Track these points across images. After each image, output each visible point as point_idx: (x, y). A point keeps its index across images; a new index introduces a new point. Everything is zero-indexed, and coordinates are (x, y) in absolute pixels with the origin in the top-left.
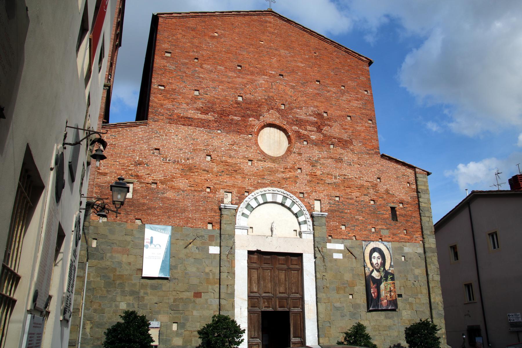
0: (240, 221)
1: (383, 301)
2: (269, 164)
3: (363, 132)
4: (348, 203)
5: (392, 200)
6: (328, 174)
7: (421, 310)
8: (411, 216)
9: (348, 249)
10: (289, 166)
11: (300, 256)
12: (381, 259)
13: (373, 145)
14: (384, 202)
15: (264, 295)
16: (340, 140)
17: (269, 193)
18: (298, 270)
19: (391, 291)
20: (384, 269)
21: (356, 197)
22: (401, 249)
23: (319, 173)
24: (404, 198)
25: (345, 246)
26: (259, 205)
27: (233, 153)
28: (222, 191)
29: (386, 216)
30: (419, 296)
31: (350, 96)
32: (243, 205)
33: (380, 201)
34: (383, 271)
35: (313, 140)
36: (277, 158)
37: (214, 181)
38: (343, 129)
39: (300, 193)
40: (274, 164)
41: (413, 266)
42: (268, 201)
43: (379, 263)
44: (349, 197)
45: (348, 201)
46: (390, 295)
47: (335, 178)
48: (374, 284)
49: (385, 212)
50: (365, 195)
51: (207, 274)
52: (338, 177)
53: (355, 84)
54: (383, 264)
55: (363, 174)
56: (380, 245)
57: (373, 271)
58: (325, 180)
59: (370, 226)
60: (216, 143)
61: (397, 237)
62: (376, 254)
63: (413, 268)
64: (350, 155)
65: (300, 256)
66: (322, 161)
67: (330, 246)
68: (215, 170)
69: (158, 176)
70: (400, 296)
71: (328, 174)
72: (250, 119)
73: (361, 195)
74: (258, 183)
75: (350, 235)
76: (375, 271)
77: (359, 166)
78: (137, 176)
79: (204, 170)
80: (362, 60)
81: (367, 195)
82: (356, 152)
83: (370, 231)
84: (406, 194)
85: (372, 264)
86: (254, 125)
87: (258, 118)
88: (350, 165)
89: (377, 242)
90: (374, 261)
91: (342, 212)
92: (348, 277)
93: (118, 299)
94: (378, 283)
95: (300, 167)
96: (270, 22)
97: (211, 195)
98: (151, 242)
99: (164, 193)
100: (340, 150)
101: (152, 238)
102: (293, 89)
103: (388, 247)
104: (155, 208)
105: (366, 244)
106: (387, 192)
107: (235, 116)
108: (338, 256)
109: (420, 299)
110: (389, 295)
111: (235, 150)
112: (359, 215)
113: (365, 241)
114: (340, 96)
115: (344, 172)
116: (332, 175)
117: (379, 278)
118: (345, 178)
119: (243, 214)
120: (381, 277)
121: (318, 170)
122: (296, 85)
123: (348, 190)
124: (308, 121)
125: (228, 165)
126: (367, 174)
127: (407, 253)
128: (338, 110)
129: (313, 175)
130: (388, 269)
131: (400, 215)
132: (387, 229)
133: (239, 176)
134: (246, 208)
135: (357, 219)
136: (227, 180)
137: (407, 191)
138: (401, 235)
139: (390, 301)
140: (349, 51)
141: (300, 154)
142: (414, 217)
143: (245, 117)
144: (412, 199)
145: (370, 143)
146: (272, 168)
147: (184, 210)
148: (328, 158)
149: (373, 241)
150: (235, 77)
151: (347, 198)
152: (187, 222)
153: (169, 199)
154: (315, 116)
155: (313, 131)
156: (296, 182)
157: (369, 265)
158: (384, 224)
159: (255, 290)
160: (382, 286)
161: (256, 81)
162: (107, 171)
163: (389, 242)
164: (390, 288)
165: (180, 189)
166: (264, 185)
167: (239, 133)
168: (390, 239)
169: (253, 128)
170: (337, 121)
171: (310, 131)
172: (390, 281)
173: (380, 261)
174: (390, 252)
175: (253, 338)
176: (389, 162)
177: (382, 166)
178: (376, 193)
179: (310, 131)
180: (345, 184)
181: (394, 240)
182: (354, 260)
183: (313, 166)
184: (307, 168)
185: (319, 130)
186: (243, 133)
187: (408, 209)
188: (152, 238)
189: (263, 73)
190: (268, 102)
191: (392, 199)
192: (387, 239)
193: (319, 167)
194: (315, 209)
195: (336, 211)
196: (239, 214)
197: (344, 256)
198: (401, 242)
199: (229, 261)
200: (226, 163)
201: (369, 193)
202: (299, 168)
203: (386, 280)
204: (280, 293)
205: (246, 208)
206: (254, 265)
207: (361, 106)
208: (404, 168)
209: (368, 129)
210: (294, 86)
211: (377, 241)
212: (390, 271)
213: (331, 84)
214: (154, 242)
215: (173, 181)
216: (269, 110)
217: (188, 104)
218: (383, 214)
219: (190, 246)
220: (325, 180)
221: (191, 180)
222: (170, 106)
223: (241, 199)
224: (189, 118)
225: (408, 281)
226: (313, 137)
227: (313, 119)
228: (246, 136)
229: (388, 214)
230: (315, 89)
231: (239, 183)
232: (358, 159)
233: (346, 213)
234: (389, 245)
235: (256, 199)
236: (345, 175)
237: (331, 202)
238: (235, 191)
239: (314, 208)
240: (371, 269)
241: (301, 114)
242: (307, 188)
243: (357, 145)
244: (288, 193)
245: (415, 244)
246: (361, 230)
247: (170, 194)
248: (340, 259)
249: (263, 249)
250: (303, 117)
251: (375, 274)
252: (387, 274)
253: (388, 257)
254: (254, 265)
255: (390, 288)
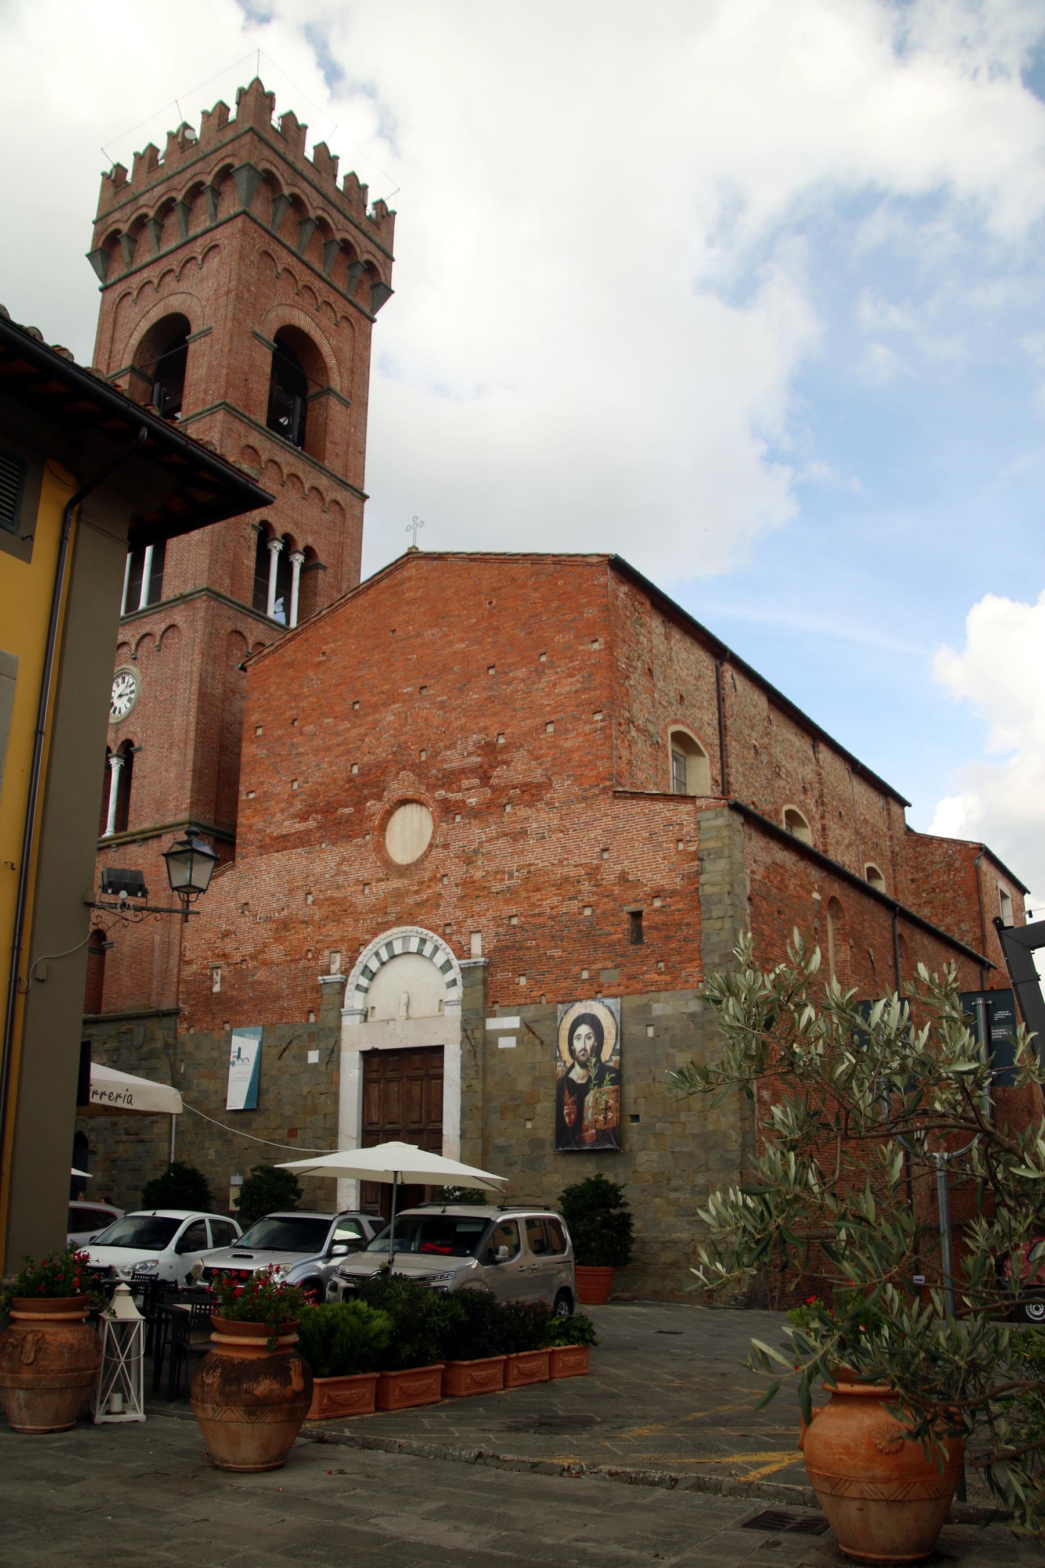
0: (354, 1000)
1: (587, 1131)
2: (396, 883)
3: (579, 749)
4: (535, 925)
5: (633, 895)
6: (497, 873)
7: (685, 1149)
8: (679, 925)
9: (526, 1025)
10: (427, 875)
11: (440, 1049)
12: (593, 1039)
13: (599, 773)
14: (612, 904)
15: (388, 1126)
16: (525, 788)
17: (412, 934)
18: (379, 1082)
19: (607, 1108)
20: (599, 1059)
21: (552, 908)
22: (647, 1008)
23: (478, 874)
24: (663, 882)
25: (522, 1020)
26: (383, 964)
27: (340, 880)
28: (326, 953)
29: (615, 937)
30: (683, 1117)
31: (557, 673)
32: (356, 971)
33: (605, 904)
34: (595, 1065)
35: (473, 808)
36: (408, 867)
37: (316, 938)
38: (534, 760)
39: (446, 925)
40: (402, 881)
41: (673, 1046)
42: (411, 950)
43: (588, 1048)
44: (536, 911)
45: (533, 920)
46: (605, 1118)
47: (511, 876)
48: (571, 1095)
49: (612, 929)
50: (570, 899)
51: (305, 1097)
52: (516, 874)
53: (570, 636)
54: (597, 1050)
55: (569, 852)
56: (597, 1008)
57: (573, 1066)
58: (489, 888)
59: (578, 968)
60: (318, 868)
61: (638, 982)
62: (584, 1030)
63: (672, 1051)
64: (543, 815)
65: (440, 1049)
66: (490, 847)
67: (493, 1024)
68: (317, 918)
69: (248, 949)
70: (635, 1118)
71: (497, 873)
72: (368, 804)
73: (563, 901)
74: (378, 924)
75: (533, 994)
76: (577, 1066)
77: (561, 835)
78: (225, 956)
79: (303, 922)
80: (592, 565)
81: (575, 898)
82: (557, 804)
83: (577, 978)
84: (671, 871)
85: (572, 1052)
86: (373, 815)
87: (379, 797)
88: (543, 838)
89: (590, 1002)
90: (578, 1045)
91: (521, 948)
92: (523, 1084)
93: (207, 1145)
94: (580, 1091)
95: (446, 871)
96: (409, 579)
97: (312, 963)
98: (239, 1057)
99: (253, 975)
100: (523, 812)
101: (240, 1049)
102: (442, 708)
103: (613, 1010)
104: (244, 1002)
105: (565, 1009)
106: (623, 878)
107: (347, 807)
108: (507, 1043)
109: (684, 1123)
110: (601, 1118)
111: (345, 872)
112: (555, 947)
113: (563, 1002)
114: (533, 683)
115: (530, 858)
116: (504, 872)
117: (583, 1081)
118: (529, 872)
119: (358, 987)
120: (589, 1080)
121: (478, 868)
122: (449, 698)
123: (538, 896)
124: (464, 769)
125: (333, 904)
126: (578, 848)
127: (660, 1018)
128: (527, 718)
129: (467, 883)
130: (607, 1058)
131: (650, 927)
132: (616, 967)
133: (349, 921)
134: (363, 973)
135: (552, 957)
136: (334, 931)
137: (673, 863)
138: (648, 976)
139: (602, 1131)
140: (560, 558)
141: (446, 846)
142: (688, 924)
143: (359, 804)
144: (686, 881)
145: (592, 770)
146: (399, 889)
147: (278, 997)
148: (497, 838)
149: (580, 1000)
150: (349, 729)
151: (532, 915)
152: (282, 1015)
153: (260, 983)
154: (479, 752)
155: (473, 788)
156: (438, 906)
157: (566, 1056)
158: (610, 958)
159: (375, 1119)
160: (589, 1099)
161: (380, 721)
162: (193, 956)
163: (616, 997)
164: (607, 1102)
165: (273, 963)
166: (386, 926)
167: (349, 838)
168: (622, 988)
169: (371, 821)
170: (522, 746)
171: (467, 789)
172: (608, 1087)
173: (590, 1044)
174: (614, 1018)
175: (370, 1203)
176: (634, 802)
177: (614, 818)
178: (595, 889)
179: (467, 789)
180: (530, 886)
181: (629, 990)
182: (539, 1046)
183: (468, 864)
184: (456, 870)
185: (485, 779)
186: (357, 836)
187: (673, 908)
188: (240, 1049)
189: (392, 698)
190: (399, 757)
191: (631, 894)
192: (614, 991)
193: (479, 863)
194: (472, 951)
195: (508, 948)
196: (350, 988)
197: (518, 1042)
198: (647, 992)
199: (328, 1074)
200: (332, 901)
201: (579, 892)
202: (443, 876)
203: (600, 1085)
204: (413, 1123)
205: (363, 973)
206: (374, 1075)
207: (579, 685)
208: (672, 805)
209: (590, 738)
210: (444, 702)
211: (593, 998)
212: (611, 1064)
213: (517, 662)
214: (242, 1056)
215: (264, 952)
216: (398, 773)
217: (282, 811)
218: (609, 934)
219: (285, 1054)
220: (489, 888)
221: (287, 943)
222: (260, 825)
223: (352, 962)
224: (285, 836)
225: (657, 1085)
226: (473, 801)
227: (476, 760)
228: (359, 841)
229: (619, 931)
230: (484, 689)
231: (350, 932)
232: (561, 819)
233: (529, 948)
234: (614, 1003)
235: (377, 954)
236: (530, 865)
237: (501, 930)
238: (344, 947)
239: (470, 950)
240: (569, 1061)
241: (453, 760)
242: (458, 913)
243: (562, 786)
244: (426, 931)
245: (683, 992)
246: (556, 980)
247: (261, 975)
248: (510, 1049)
249: (381, 1046)
250: (456, 764)
251: (578, 1075)
252: (603, 1069)
253: (609, 1033)
254: (374, 1075)
255: (607, 1102)
